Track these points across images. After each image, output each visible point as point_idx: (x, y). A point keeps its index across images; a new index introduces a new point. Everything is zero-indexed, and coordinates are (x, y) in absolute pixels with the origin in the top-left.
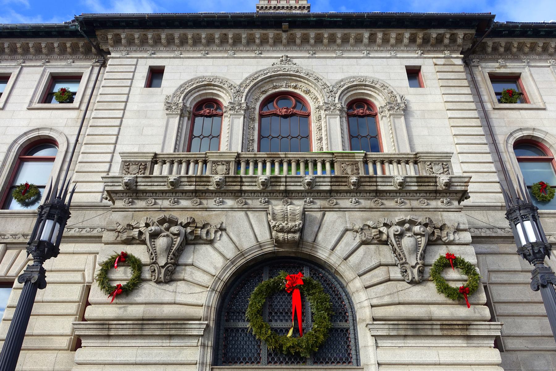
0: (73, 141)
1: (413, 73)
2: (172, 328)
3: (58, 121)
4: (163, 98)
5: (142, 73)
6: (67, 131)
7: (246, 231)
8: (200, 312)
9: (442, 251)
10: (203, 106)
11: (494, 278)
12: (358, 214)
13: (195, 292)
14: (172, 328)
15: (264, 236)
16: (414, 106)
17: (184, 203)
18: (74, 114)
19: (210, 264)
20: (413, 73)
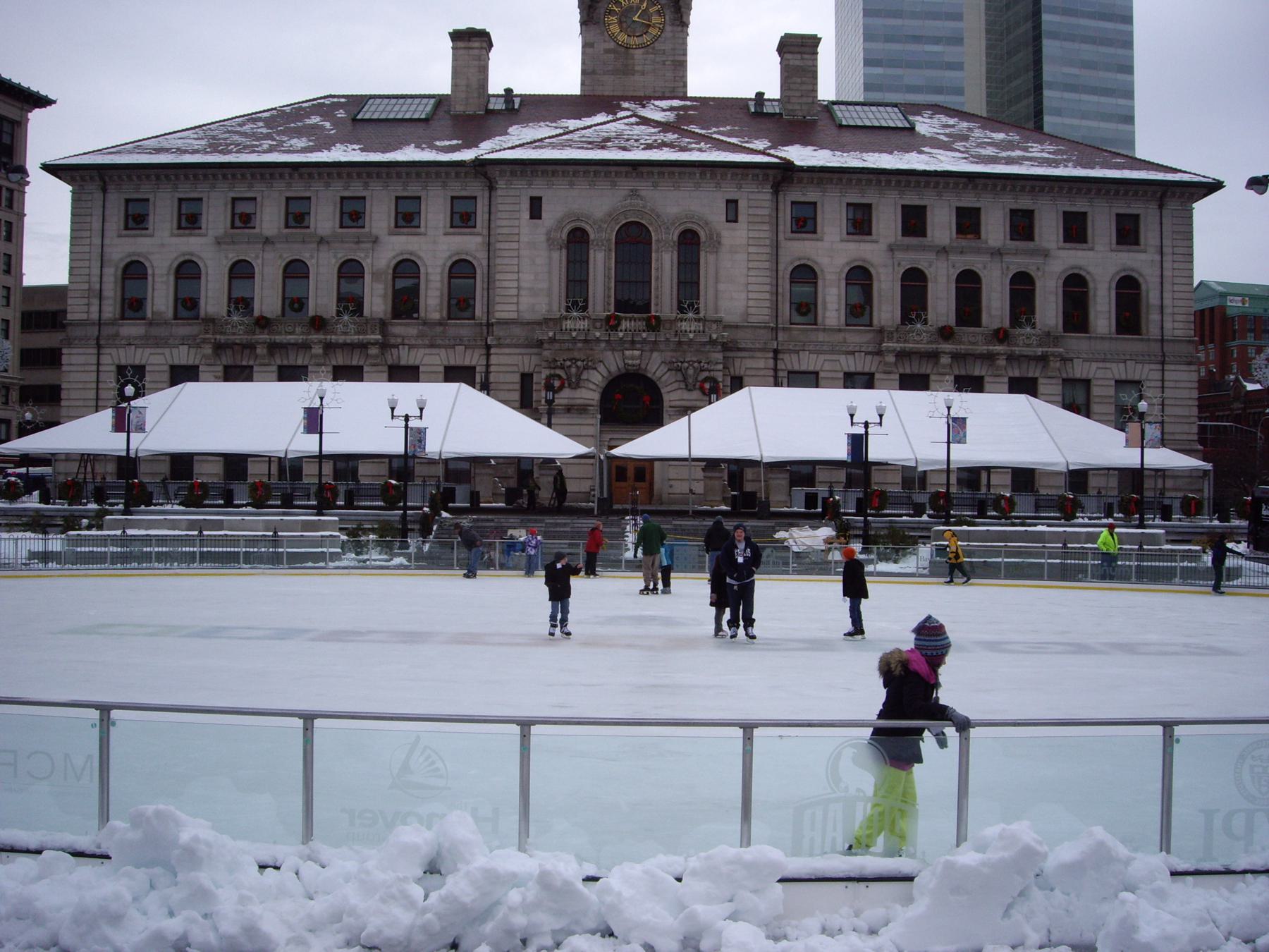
0: (485, 263)
1: (732, 204)
2: (582, 409)
3: (469, 244)
4: (544, 230)
5: (526, 205)
6: (479, 255)
7: (612, 363)
8: (594, 403)
9: (705, 374)
10: (577, 241)
11: (748, 372)
12: (669, 354)
13: (590, 394)
14: (582, 409)
15: (621, 365)
16: (724, 241)
17: (580, 345)
18: (479, 239)
19: (597, 378)
20: (732, 204)
